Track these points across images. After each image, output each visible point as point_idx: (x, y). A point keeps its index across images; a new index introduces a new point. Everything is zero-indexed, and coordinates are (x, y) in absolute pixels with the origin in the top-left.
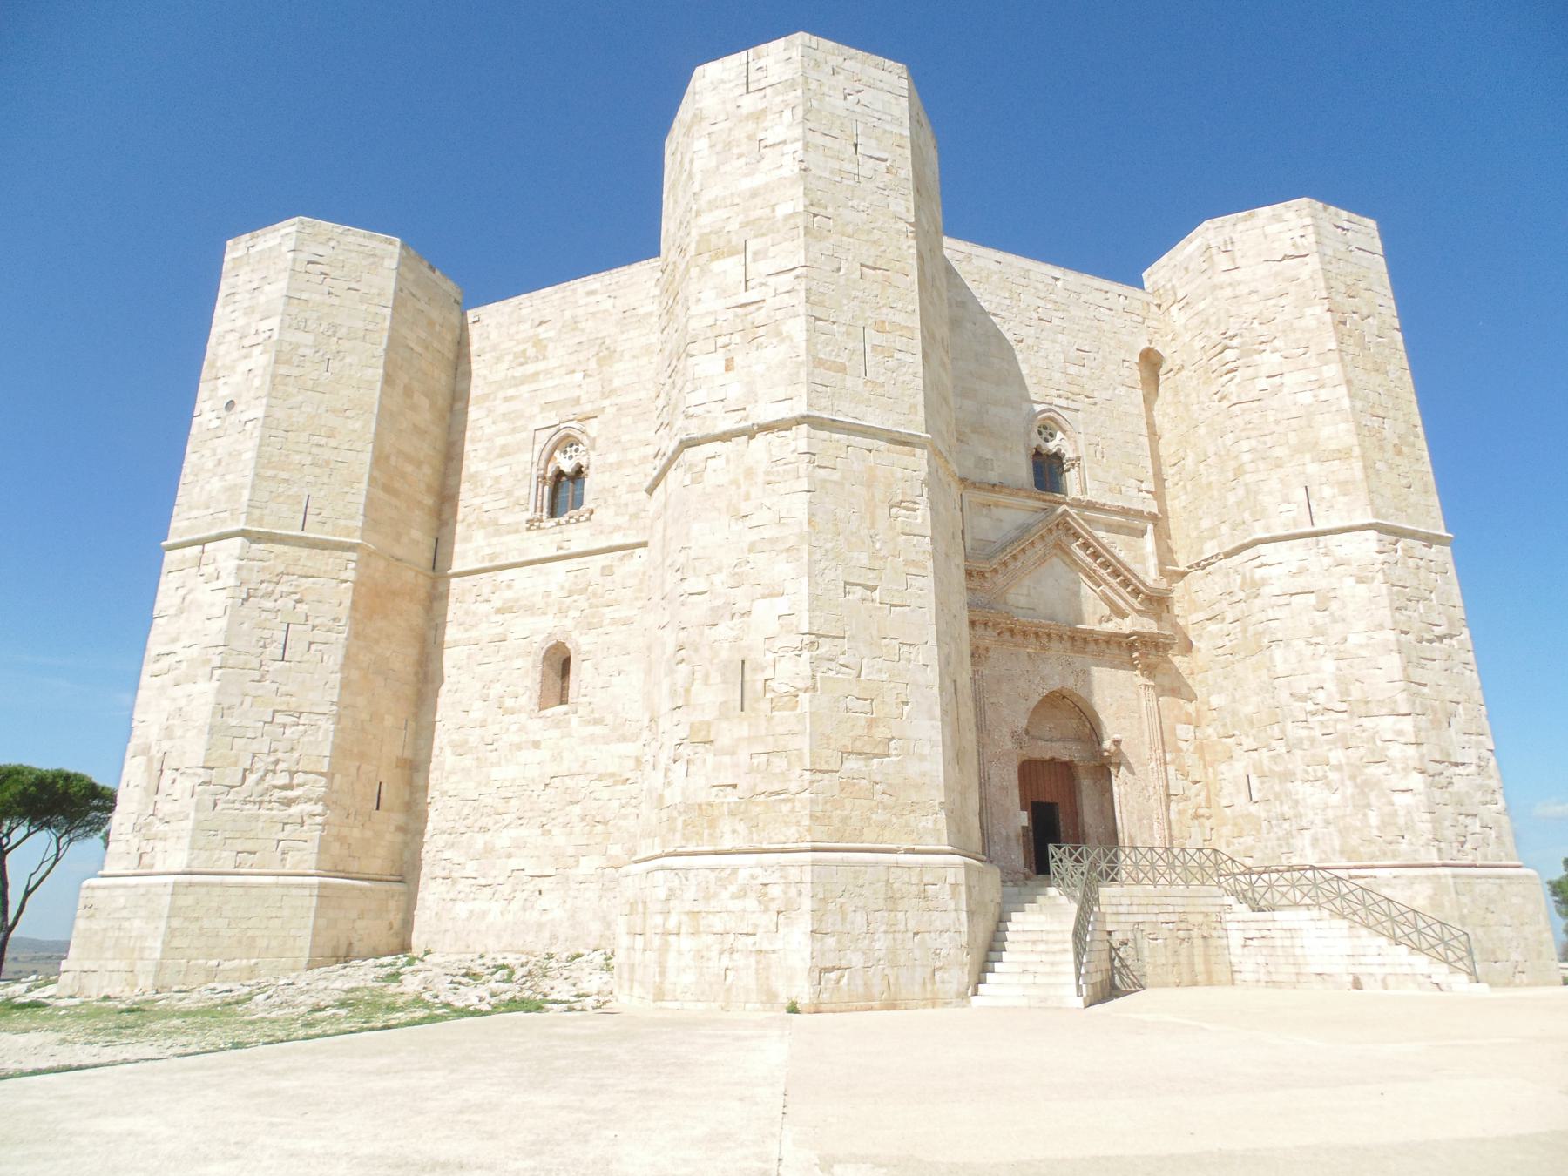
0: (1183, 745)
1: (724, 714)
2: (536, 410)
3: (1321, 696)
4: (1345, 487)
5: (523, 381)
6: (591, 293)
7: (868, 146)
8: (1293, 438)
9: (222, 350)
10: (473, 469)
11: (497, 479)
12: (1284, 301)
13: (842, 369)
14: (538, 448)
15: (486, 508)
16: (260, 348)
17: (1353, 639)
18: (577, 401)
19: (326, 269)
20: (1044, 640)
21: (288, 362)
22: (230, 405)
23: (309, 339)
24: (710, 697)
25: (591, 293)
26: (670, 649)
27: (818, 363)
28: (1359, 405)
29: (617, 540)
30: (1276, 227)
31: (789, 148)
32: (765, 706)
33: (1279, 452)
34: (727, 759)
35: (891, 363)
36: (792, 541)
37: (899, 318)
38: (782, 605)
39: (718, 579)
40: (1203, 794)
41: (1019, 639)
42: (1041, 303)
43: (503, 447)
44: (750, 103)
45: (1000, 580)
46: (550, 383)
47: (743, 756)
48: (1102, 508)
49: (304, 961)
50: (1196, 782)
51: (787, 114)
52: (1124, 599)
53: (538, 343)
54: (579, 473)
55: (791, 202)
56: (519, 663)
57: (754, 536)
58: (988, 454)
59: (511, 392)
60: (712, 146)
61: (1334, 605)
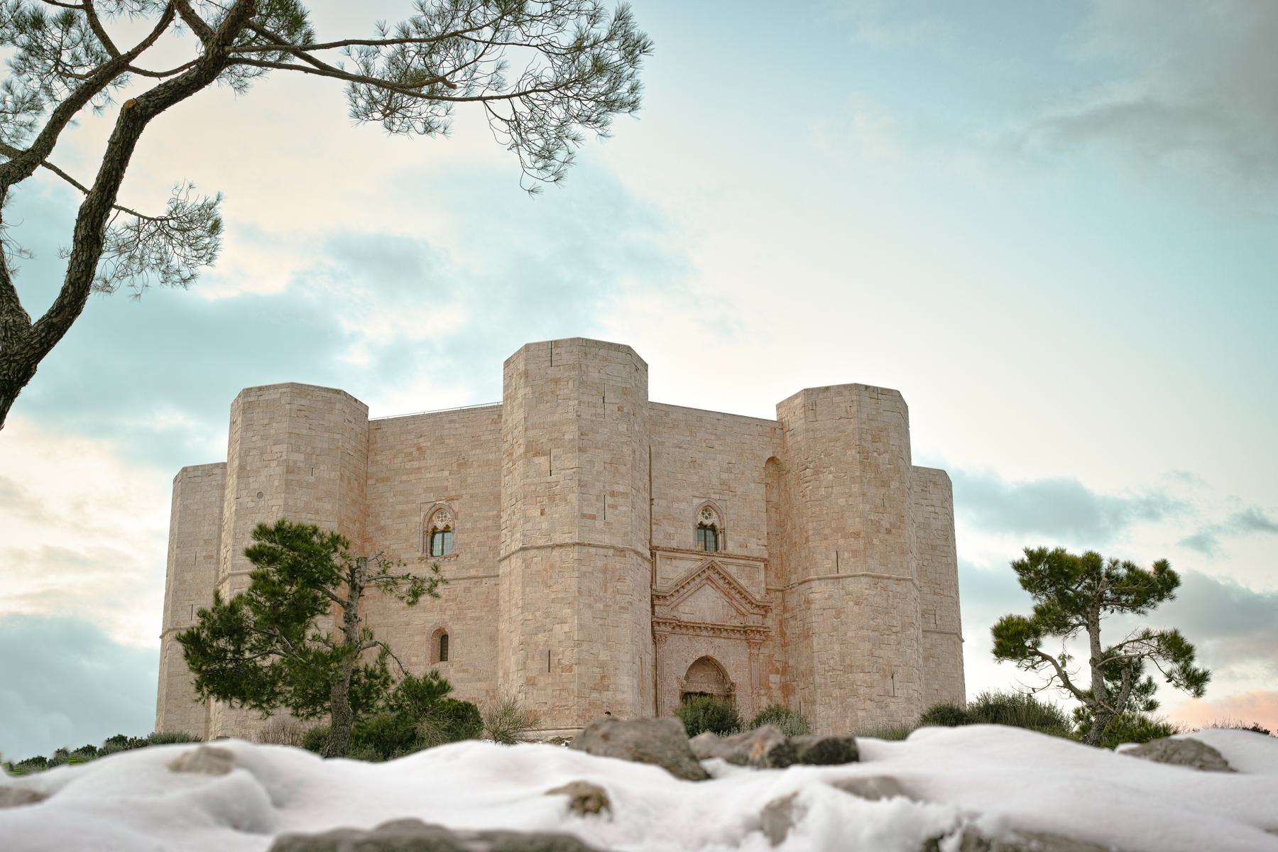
0: (773, 686)
1: (541, 674)
2: (420, 491)
3: (832, 662)
4: (855, 553)
5: (412, 471)
6: (451, 422)
7: (610, 397)
8: (834, 525)
9: (249, 459)
10: (382, 523)
11: (398, 531)
12: (838, 444)
13: (594, 517)
15: (393, 547)
16: (274, 464)
17: (850, 634)
19: (307, 413)
21: (293, 472)
22: (260, 495)
23: (300, 457)
24: (535, 666)
25: (451, 422)
26: (515, 643)
27: (584, 516)
28: (868, 507)
29: (473, 572)
30: (836, 399)
31: (571, 403)
32: (559, 670)
33: (827, 531)
35: (617, 512)
36: (570, 600)
37: (622, 489)
39: (538, 614)
41: (684, 631)
42: (707, 436)
43: (401, 512)
44: (552, 372)
45: (673, 599)
46: (429, 476)
47: (549, 691)
51: (571, 383)
53: (419, 449)
54: (446, 530)
55: (571, 433)
56: (417, 638)
57: (553, 596)
58: (672, 530)
59: (404, 478)
60: (534, 393)
61: (843, 616)
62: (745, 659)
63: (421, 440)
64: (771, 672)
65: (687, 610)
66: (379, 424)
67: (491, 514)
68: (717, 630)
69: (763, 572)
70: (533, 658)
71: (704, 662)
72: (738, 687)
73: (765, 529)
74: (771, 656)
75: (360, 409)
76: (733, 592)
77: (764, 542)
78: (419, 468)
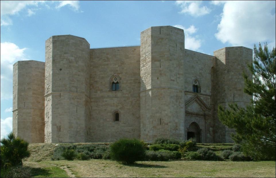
6: (118, 50)
10: (96, 80)
11: (101, 82)
14: (109, 78)
18: (117, 71)
20: (192, 115)
29: (127, 95)
32: (164, 124)
34: (158, 130)
38: (166, 112)
41: (189, 115)
48: (203, 95)
49: (108, 153)
53: (108, 58)
63: (108, 56)
66: (93, 50)
67: (132, 79)
68: (197, 115)
70: (155, 121)
71: (194, 124)
73: (210, 87)
75: (88, 45)
76: (202, 104)
77: (210, 91)
78: (108, 64)
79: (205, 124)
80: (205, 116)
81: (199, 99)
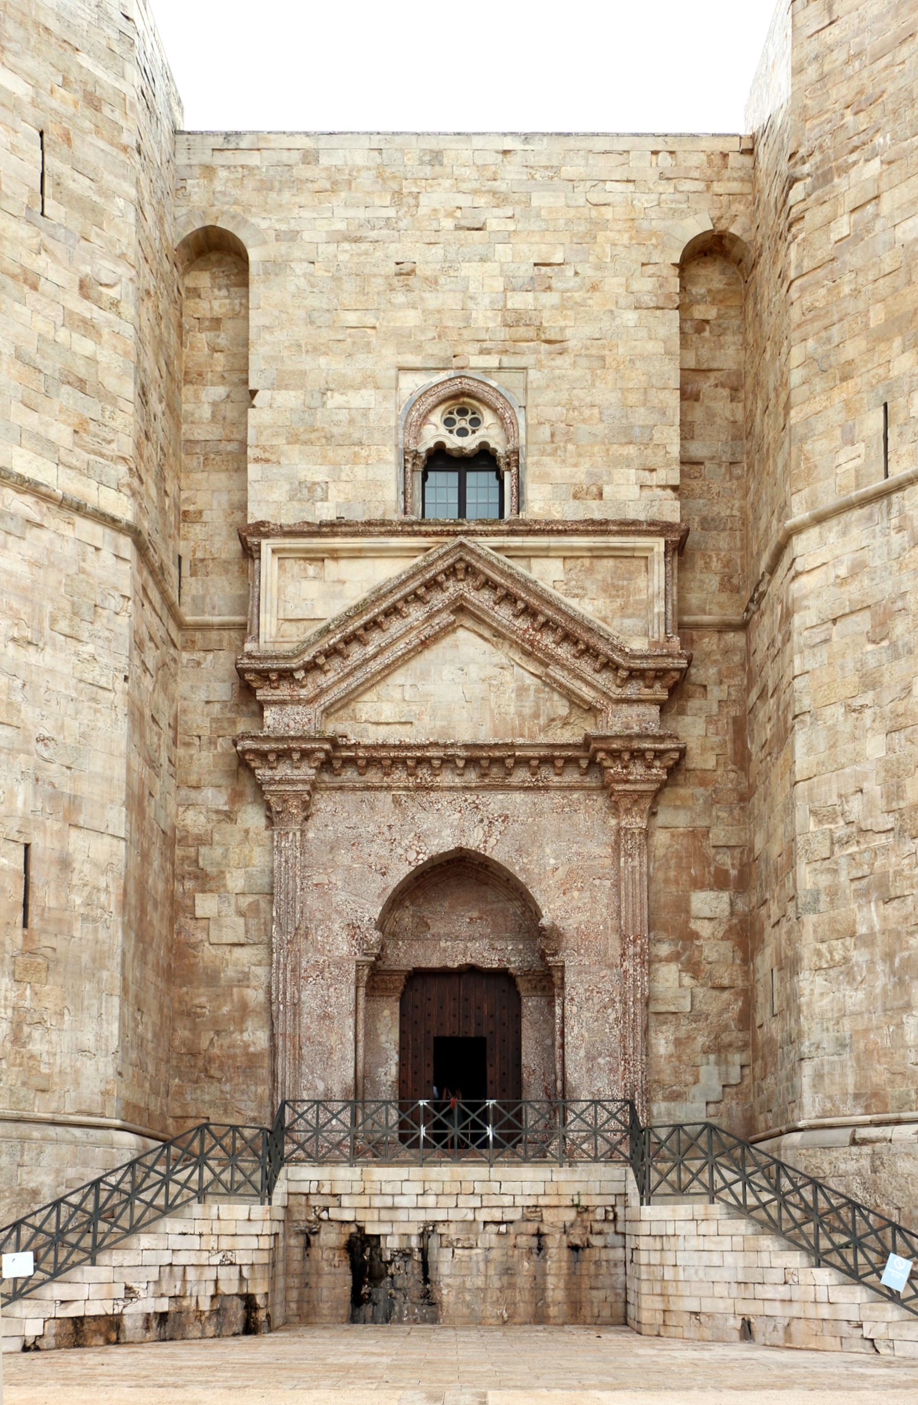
0: (704, 929)
20: (424, 773)
40: (737, 1006)
41: (374, 777)
50: (723, 988)
52: (594, 684)
62: (599, 850)
64: (698, 884)
65: (388, 712)
68: (489, 763)
69: (659, 569)
72: (571, 939)
74: (697, 835)
76: (547, 640)
79: (616, 847)
80: (590, 760)
81: (489, 584)
